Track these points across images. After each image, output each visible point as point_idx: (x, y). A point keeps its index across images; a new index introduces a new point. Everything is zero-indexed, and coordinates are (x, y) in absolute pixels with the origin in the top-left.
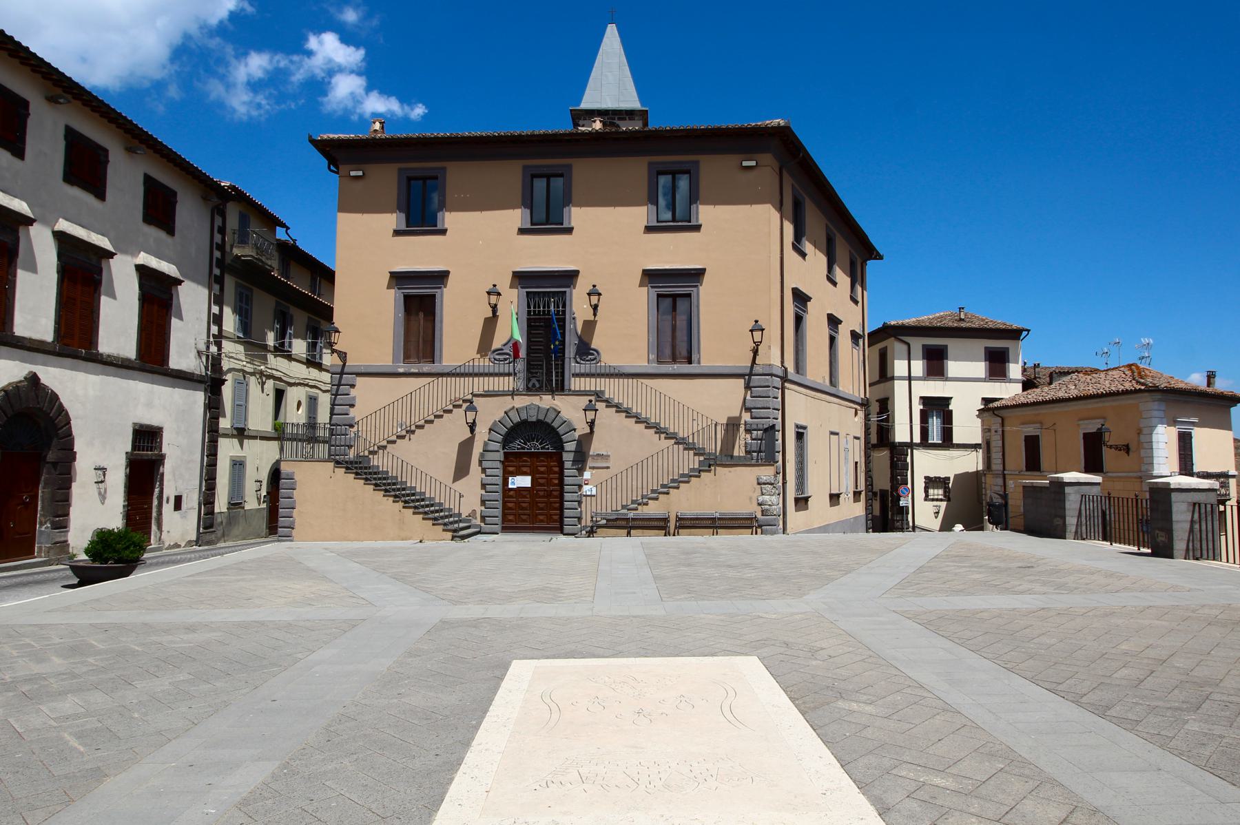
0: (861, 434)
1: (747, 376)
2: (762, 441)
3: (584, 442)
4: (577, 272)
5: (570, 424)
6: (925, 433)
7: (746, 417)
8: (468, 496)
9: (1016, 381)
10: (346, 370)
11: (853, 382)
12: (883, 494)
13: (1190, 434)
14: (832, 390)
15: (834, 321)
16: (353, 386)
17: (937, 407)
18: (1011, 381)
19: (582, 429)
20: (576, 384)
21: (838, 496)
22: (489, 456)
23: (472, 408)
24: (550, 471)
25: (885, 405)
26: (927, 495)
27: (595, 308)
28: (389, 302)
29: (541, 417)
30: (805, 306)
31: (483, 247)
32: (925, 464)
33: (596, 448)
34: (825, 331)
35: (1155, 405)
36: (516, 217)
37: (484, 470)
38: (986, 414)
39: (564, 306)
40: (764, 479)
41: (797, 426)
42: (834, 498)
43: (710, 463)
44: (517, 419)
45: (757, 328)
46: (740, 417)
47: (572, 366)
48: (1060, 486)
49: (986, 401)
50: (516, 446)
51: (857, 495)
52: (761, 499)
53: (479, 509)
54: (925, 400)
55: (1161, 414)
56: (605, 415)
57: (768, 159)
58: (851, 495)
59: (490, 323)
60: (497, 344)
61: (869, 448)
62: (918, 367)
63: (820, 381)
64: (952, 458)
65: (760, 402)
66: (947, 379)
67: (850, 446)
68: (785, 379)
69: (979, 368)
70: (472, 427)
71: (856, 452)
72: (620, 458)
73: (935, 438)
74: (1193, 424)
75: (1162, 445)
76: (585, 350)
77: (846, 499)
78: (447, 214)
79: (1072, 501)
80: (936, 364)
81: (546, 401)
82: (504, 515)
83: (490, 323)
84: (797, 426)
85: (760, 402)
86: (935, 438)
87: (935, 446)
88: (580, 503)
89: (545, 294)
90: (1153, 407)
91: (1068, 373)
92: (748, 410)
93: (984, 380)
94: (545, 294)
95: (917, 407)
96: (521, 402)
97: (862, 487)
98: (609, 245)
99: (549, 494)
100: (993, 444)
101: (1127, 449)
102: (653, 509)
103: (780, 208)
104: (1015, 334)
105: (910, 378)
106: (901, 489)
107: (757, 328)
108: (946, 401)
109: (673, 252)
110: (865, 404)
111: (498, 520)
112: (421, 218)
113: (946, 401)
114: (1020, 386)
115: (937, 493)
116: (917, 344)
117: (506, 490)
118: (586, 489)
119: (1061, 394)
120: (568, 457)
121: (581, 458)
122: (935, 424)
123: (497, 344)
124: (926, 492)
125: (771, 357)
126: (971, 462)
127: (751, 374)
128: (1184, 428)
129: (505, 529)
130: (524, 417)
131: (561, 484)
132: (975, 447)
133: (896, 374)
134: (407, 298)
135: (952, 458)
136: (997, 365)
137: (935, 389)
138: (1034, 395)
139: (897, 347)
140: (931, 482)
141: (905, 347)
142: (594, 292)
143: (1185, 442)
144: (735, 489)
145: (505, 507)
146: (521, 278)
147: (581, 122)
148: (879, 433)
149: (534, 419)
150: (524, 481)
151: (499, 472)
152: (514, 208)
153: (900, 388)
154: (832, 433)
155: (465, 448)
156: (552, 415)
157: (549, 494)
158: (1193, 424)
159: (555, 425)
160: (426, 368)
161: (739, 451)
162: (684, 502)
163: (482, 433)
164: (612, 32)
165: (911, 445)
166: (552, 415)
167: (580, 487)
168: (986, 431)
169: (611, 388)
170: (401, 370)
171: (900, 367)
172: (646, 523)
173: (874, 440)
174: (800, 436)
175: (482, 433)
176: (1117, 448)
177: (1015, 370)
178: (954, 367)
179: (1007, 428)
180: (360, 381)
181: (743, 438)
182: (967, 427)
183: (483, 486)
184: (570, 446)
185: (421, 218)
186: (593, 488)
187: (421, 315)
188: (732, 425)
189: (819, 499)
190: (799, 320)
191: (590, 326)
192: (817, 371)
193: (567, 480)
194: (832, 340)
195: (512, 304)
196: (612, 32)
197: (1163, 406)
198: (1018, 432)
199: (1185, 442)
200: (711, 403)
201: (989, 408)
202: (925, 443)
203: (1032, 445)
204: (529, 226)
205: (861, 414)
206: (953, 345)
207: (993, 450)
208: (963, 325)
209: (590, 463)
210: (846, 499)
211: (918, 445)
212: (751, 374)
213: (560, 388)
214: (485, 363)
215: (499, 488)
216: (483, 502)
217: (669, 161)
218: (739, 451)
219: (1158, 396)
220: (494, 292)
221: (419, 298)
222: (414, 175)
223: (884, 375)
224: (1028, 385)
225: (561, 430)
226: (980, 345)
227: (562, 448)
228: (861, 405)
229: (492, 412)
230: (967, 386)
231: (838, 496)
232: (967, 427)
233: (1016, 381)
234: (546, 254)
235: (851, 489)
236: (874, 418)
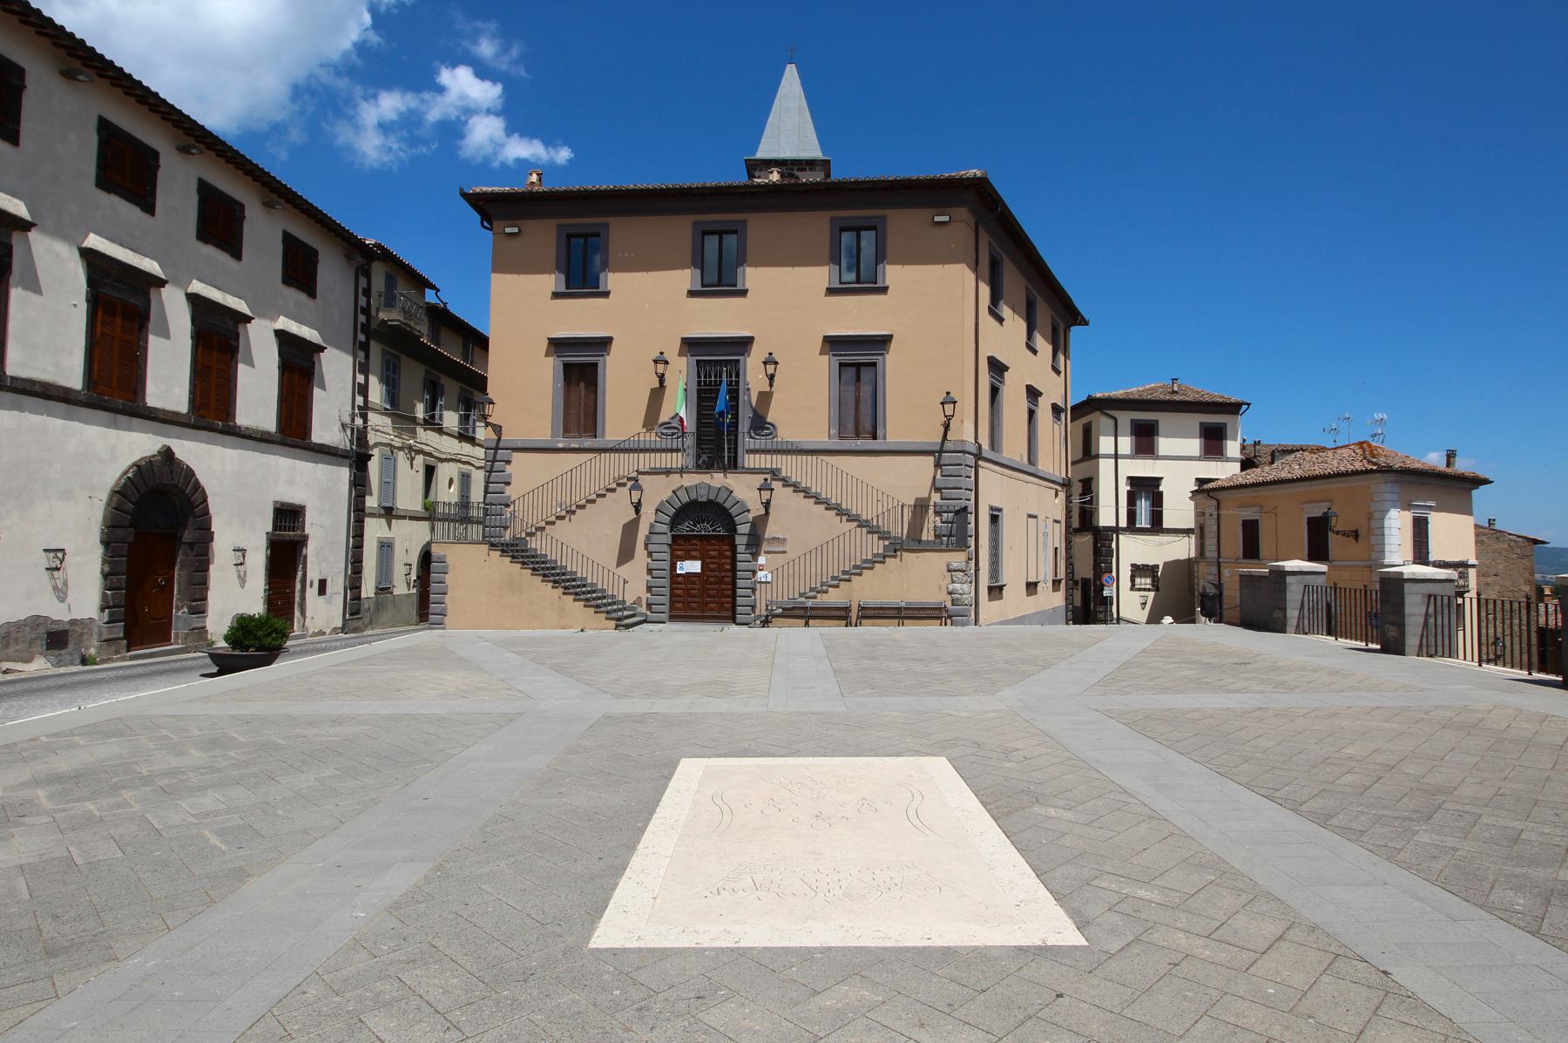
0: (1061, 516)
1: (937, 453)
2: (954, 526)
3: (758, 525)
4: (752, 339)
5: (743, 504)
7: (936, 498)
8: (633, 582)
9: (1233, 460)
10: (501, 445)
11: (1054, 458)
12: (1085, 582)
13: (1425, 520)
14: (1031, 469)
15: (1033, 394)
16: (508, 462)
17: (1146, 488)
19: (756, 509)
20: (750, 461)
21: (1035, 584)
22: (656, 538)
23: (637, 486)
24: (721, 554)
25: (1089, 486)
26: (1133, 585)
27: (771, 378)
28: (547, 371)
29: (712, 497)
30: (1002, 376)
31: (649, 311)
32: (1133, 550)
33: (771, 530)
34: (1023, 403)
35: (1388, 487)
36: (686, 278)
37: (650, 554)
38: (1200, 496)
39: (737, 376)
40: (955, 565)
41: (992, 508)
42: (1032, 587)
43: (896, 548)
44: (685, 499)
45: (949, 400)
46: (929, 498)
47: (746, 441)
48: (1281, 575)
49: (1201, 482)
50: (685, 528)
51: (1056, 583)
52: (951, 587)
53: (645, 596)
54: (1134, 481)
55: (1395, 497)
56: (781, 494)
57: (962, 213)
58: (1050, 584)
60: (661, 420)
61: (1070, 532)
62: (1126, 444)
63: (1018, 459)
64: (1161, 544)
65: (952, 481)
66: (1158, 458)
67: (1049, 530)
68: (979, 456)
69: (1194, 445)
70: (637, 507)
71: (1057, 536)
72: (796, 541)
73: (1143, 521)
74: (1430, 508)
75: (1394, 532)
76: (760, 424)
77: (1045, 588)
78: (610, 275)
81: (717, 479)
82: (672, 603)
84: (992, 508)
85: (952, 481)
86: (1143, 521)
87: (1143, 531)
88: (754, 590)
89: (716, 360)
90: (1384, 489)
91: (1292, 451)
92: (938, 490)
94: (716, 360)
95: (1124, 489)
96: (690, 480)
97: (1062, 574)
98: (787, 308)
99: (721, 581)
100: (1207, 529)
101: (1356, 535)
102: (833, 598)
103: (975, 268)
104: (1234, 408)
105: (1116, 456)
106: (1105, 577)
107: (949, 400)
108: (1156, 481)
109: (857, 316)
110: (1066, 484)
111: (666, 608)
112: (581, 279)
113: (1156, 481)
114: (1238, 465)
115: (1145, 582)
116: (1125, 418)
118: (761, 575)
119: (1284, 475)
120: (741, 541)
121: (755, 542)
122: (1143, 507)
123: (664, 417)
124: (1133, 581)
125: (964, 432)
126: (1183, 549)
127: (941, 451)
128: (1420, 513)
129: (673, 618)
130: (693, 497)
131: (734, 569)
132: (1188, 532)
133: (1102, 452)
134: (567, 366)
135: (1161, 544)
136: (1213, 441)
137: (1144, 468)
138: (1253, 476)
139: (1101, 421)
140: (1137, 570)
141: (1112, 422)
142: (770, 361)
143: (1420, 529)
144: (923, 576)
145: (672, 594)
146: (691, 345)
148: (1082, 520)
149: (704, 499)
150: (693, 566)
151: (667, 556)
152: (683, 268)
153: (1105, 467)
154: (1030, 516)
155: (630, 529)
156: (723, 495)
158: (1430, 508)
159: (727, 505)
161: (927, 535)
164: (791, 75)
165: (1117, 530)
166: (723, 495)
167: (754, 572)
168: (1200, 514)
169: (789, 466)
170: (560, 445)
171: (1105, 444)
172: (825, 613)
173: (1076, 523)
176: (1345, 534)
177: (1233, 448)
178: (1164, 444)
179: (1223, 512)
180: (516, 456)
181: (932, 521)
182: (1179, 509)
183: (650, 571)
184: (744, 529)
185: (581, 279)
186: (767, 574)
187: (582, 385)
188: (921, 507)
190: (995, 391)
191: (765, 397)
192: (1014, 446)
193: (740, 566)
194: (1031, 413)
195: (681, 374)
196: (791, 75)
198: (1234, 517)
199: (1420, 529)
200: (896, 483)
201: (1204, 489)
202: (1132, 528)
203: (1251, 531)
204: (699, 288)
205: (1062, 495)
206: (1164, 419)
207: (1207, 535)
208: (1176, 398)
209: (765, 547)
210: (1045, 588)
211: (1124, 530)
212: (941, 451)
213: (733, 465)
214: (651, 438)
215: (666, 573)
216: (649, 589)
217: (852, 216)
218: (927, 535)
219: (1391, 477)
220: (661, 360)
221: (580, 366)
222: (574, 230)
223: (1088, 453)
224: (1247, 464)
225: (734, 511)
226: (1195, 420)
227: (735, 531)
228: (1063, 485)
229: (658, 492)
230: (1180, 465)
231: (1035, 584)
232: (1179, 509)
233: (1233, 460)
234: (718, 318)
235: (1050, 577)
236: (1076, 500)
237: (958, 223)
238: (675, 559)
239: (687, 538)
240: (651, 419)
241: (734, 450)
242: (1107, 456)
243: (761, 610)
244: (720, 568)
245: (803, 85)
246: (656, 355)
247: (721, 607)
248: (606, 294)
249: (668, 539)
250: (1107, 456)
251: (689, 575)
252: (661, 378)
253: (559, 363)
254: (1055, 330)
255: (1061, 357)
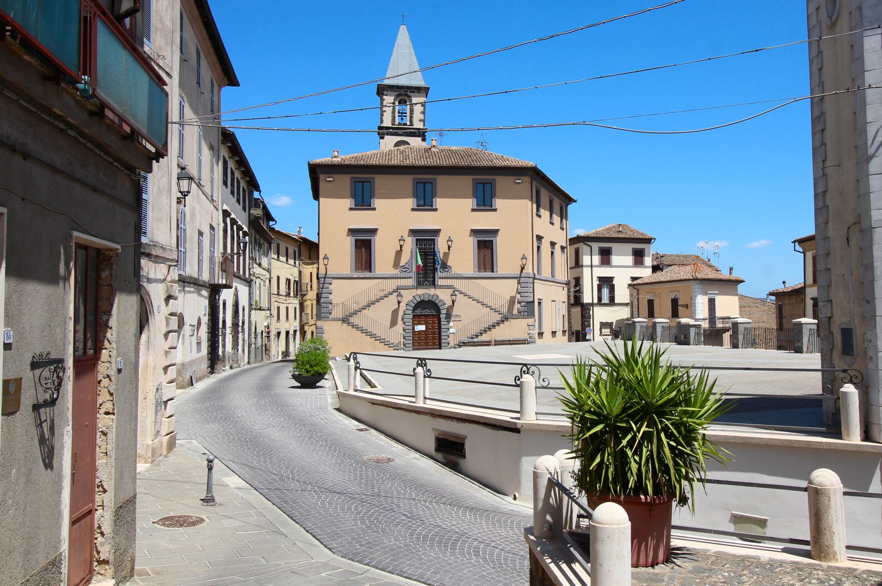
1: (519, 278)
2: (529, 309)
3: (450, 309)
6: (600, 299)
7: (518, 296)
8: (397, 334)
9: (648, 267)
11: (562, 274)
12: (578, 332)
14: (553, 279)
15: (553, 244)
17: (606, 282)
18: (646, 267)
19: (449, 303)
20: (440, 282)
22: (406, 316)
23: (400, 295)
24: (433, 322)
25: (578, 281)
27: (449, 248)
31: (394, 218)
32: (601, 315)
33: (455, 312)
34: (549, 250)
35: (697, 286)
36: (410, 202)
37: (404, 323)
42: (554, 333)
43: (505, 319)
44: (419, 300)
45: (524, 257)
47: (439, 274)
48: (634, 323)
49: (634, 279)
50: (418, 312)
51: (564, 332)
57: (527, 179)
59: (399, 253)
60: (402, 263)
61: (570, 306)
62: (596, 259)
65: (524, 290)
66: (612, 267)
68: (534, 278)
69: (629, 260)
70: (399, 303)
73: (605, 300)
76: (445, 266)
77: (559, 334)
79: (638, 327)
80: (606, 256)
81: (432, 291)
83: (399, 253)
85: (524, 290)
86: (605, 300)
87: (605, 305)
89: (426, 241)
90: (696, 287)
92: (519, 293)
93: (632, 267)
94: (426, 241)
95: (596, 283)
96: (421, 291)
97: (566, 328)
98: (454, 217)
99: (433, 333)
101: (687, 306)
102: (485, 338)
103: (531, 200)
104: (648, 241)
105: (592, 266)
106: (587, 329)
107: (524, 257)
108: (611, 279)
109: (484, 220)
110: (568, 284)
112: (363, 202)
113: (611, 279)
115: (607, 331)
116: (596, 246)
117: (414, 332)
118: (451, 331)
119: (663, 279)
120: (443, 316)
121: (449, 316)
122: (605, 292)
125: (529, 270)
126: (623, 313)
128: (711, 296)
129: (414, 349)
131: (440, 328)
132: (627, 304)
134: (356, 240)
136: (639, 256)
137: (605, 272)
138: (660, 276)
139: (584, 248)
140: (603, 325)
142: (450, 240)
143: (712, 302)
144: (517, 328)
145: (413, 340)
146: (413, 232)
147: (385, 93)
148: (576, 300)
150: (422, 328)
153: (586, 272)
155: (395, 313)
156: (435, 298)
157: (433, 333)
160: (368, 274)
161: (515, 312)
162: (498, 334)
163: (403, 306)
164: (403, 31)
165: (592, 304)
166: (435, 298)
168: (631, 295)
169: (457, 284)
171: (586, 260)
173: (572, 301)
174: (539, 303)
175: (403, 306)
176: (683, 306)
177: (648, 261)
178: (615, 259)
181: (517, 306)
182: (622, 294)
183: (404, 330)
184: (444, 311)
185: (363, 202)
186: (453, 330)
188: (512, 301)
189: (547, 334)
190: (539, 248)
191: (446, 255)
192: (546, 273)
194: (552, 253)
195: (410, 243)
196: (403, 29)
197: (701, 286)
198: (645, 297)
199: (712, 302)
200: (501, 291)
201: (635, 285)
202: (600, 303)
203: (651, 303)
205: (566, 289)
206: (615, 246)
208: (620, 236)
209: (453, 319)
210: (559, 334)
213: (433, 284)
214: (396, 272)
216: (404, 338)
217: (485, 181)
218: (515, 312)
220: (402, 239)
221: (363, 244)
222: (361, 181)
224: (656, 269)
225: (439, 304)
226: (630, 247)
227: (440, 312)
229: (409, 296)
230: (623, 269)
232: (622, 294)
234: (425, 221)
236: (572, 290)
237: (524, 184)
238: (414, 324)
239: (419, 316)
240: (396, 264)
241: (434, 277)
242: (587, 266)
243: (452, 344)
244: (433, 328)
245: (411, 38)
246: (400, 238)
247: (434, 344)
248: (374, 209)
249: (411, 316)
250: (587, 266)
251: (420, 332)
252: (401, 246)
253: (353, 239)
254: (561, 208)
255: (564, 221)
